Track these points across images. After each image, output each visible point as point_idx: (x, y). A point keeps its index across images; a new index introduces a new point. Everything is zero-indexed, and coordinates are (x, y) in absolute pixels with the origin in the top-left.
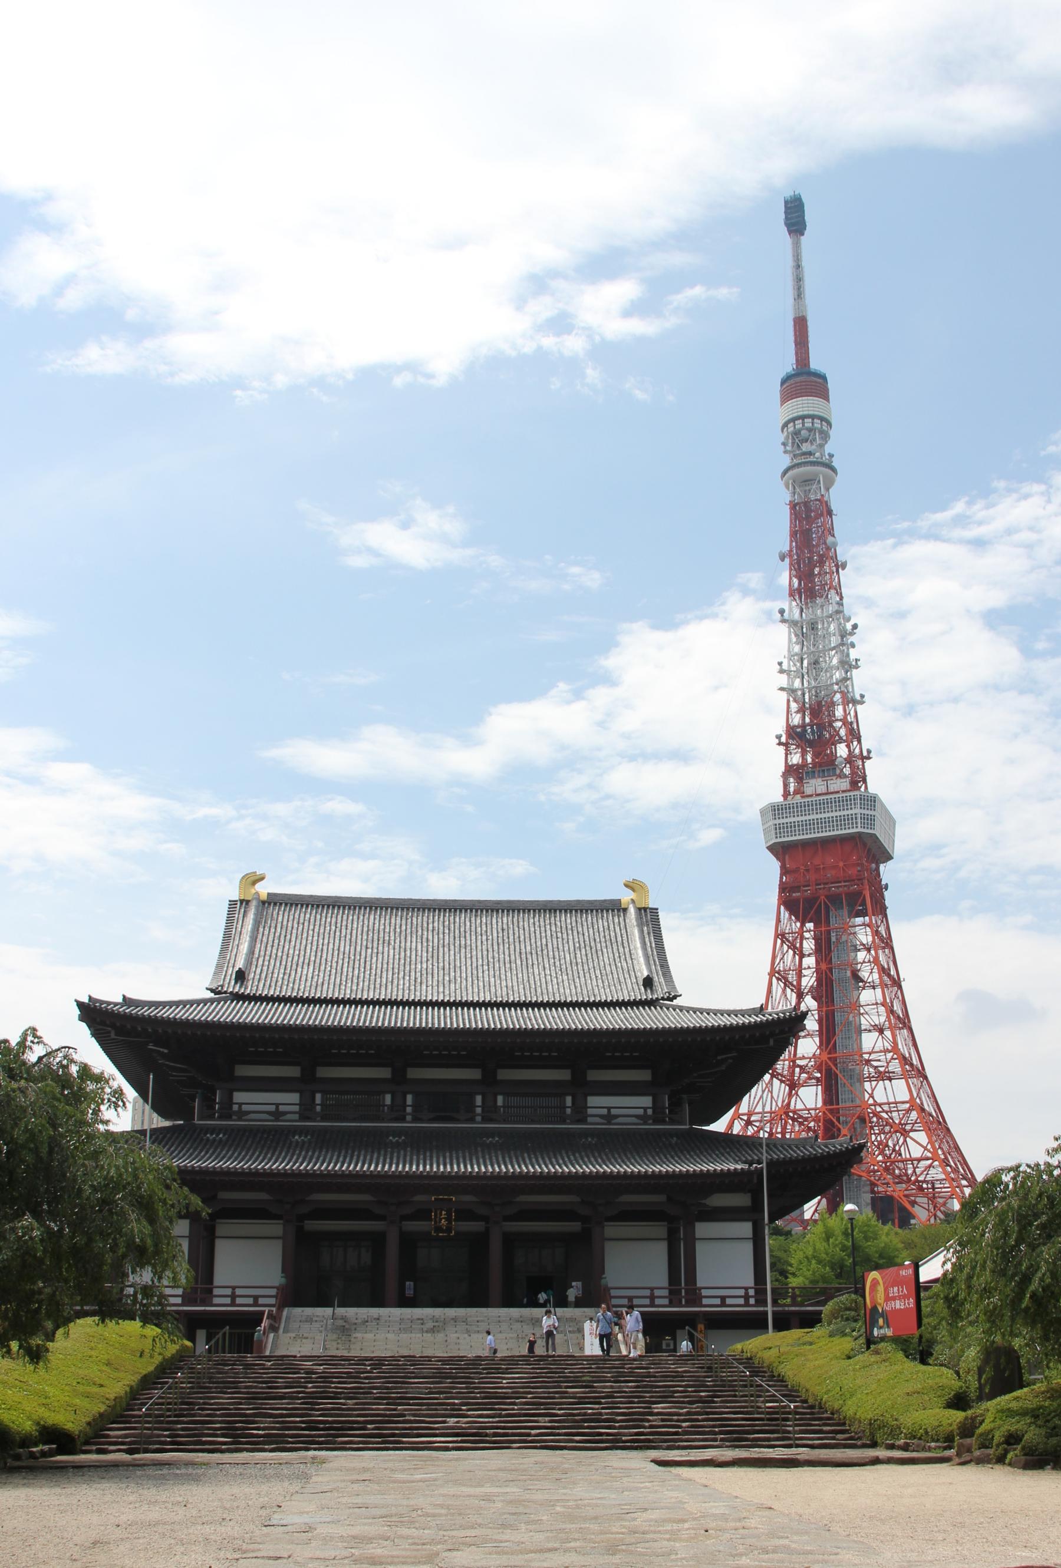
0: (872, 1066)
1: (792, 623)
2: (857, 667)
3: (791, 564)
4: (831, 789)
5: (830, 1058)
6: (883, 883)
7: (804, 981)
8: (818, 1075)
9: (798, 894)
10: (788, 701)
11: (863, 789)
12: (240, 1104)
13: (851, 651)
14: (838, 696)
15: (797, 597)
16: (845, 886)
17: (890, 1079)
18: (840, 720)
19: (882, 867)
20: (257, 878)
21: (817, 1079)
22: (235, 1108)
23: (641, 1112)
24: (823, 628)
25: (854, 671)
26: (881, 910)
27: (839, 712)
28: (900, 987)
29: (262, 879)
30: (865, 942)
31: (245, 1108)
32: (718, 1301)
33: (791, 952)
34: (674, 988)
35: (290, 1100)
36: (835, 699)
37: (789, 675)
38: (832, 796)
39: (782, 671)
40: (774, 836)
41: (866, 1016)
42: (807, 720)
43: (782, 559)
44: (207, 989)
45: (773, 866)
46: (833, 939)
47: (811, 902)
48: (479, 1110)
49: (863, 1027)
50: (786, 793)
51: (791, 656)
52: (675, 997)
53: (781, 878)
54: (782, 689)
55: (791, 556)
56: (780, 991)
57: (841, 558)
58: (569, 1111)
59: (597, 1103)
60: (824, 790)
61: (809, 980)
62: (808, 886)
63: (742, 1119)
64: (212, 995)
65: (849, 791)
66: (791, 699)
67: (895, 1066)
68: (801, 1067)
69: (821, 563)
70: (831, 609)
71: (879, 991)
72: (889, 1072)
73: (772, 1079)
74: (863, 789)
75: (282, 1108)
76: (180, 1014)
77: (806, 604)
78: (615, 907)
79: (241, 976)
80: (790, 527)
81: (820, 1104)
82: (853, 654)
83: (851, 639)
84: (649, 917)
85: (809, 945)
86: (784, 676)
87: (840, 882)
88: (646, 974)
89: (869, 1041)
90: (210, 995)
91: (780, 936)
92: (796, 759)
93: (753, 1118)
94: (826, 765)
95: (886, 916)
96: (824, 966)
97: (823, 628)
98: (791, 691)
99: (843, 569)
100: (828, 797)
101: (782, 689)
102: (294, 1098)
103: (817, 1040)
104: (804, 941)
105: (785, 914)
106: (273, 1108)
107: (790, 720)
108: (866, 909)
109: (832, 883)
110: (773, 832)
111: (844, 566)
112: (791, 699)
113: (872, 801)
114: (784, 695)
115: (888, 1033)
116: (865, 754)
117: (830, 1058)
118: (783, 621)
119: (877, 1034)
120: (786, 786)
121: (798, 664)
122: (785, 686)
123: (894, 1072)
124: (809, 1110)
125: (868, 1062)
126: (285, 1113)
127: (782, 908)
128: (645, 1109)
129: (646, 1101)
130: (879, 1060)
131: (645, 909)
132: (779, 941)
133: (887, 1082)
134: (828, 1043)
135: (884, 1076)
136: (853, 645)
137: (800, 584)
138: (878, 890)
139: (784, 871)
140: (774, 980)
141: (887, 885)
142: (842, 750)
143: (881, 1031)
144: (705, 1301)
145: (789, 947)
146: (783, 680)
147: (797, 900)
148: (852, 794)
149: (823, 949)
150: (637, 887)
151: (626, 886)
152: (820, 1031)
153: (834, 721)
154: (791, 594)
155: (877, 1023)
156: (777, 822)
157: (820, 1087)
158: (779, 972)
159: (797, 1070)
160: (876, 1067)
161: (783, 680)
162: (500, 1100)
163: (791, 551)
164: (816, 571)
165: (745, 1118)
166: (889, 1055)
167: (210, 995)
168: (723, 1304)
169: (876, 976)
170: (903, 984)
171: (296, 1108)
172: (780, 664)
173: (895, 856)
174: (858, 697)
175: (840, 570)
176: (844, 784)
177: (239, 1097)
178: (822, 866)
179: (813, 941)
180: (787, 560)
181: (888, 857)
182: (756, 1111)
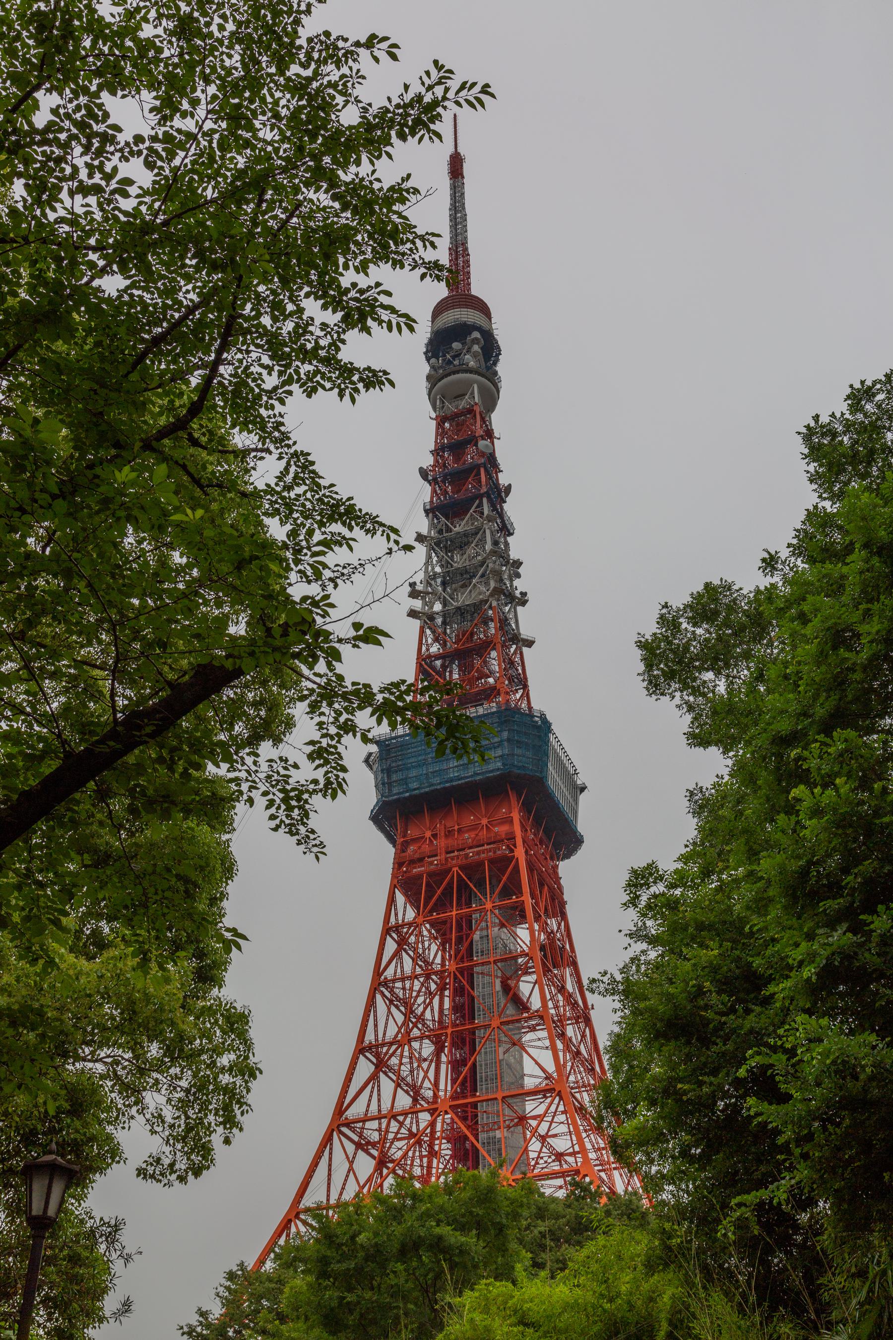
2: (523, 603)
16: (490, 850)
25: (519, 609)
28: (588, 1021)
37: (423, 598)
49: (530, 1083)
51: (430, 578)
62: (436, 855)
98: (426, 618)
99: (507, 494)
101: (413, 614)
107: (424, 648)
109: (471, 848)
114: (416, 624)
158: (385, 983)
170: (592, 1012)
178: (456, 827)
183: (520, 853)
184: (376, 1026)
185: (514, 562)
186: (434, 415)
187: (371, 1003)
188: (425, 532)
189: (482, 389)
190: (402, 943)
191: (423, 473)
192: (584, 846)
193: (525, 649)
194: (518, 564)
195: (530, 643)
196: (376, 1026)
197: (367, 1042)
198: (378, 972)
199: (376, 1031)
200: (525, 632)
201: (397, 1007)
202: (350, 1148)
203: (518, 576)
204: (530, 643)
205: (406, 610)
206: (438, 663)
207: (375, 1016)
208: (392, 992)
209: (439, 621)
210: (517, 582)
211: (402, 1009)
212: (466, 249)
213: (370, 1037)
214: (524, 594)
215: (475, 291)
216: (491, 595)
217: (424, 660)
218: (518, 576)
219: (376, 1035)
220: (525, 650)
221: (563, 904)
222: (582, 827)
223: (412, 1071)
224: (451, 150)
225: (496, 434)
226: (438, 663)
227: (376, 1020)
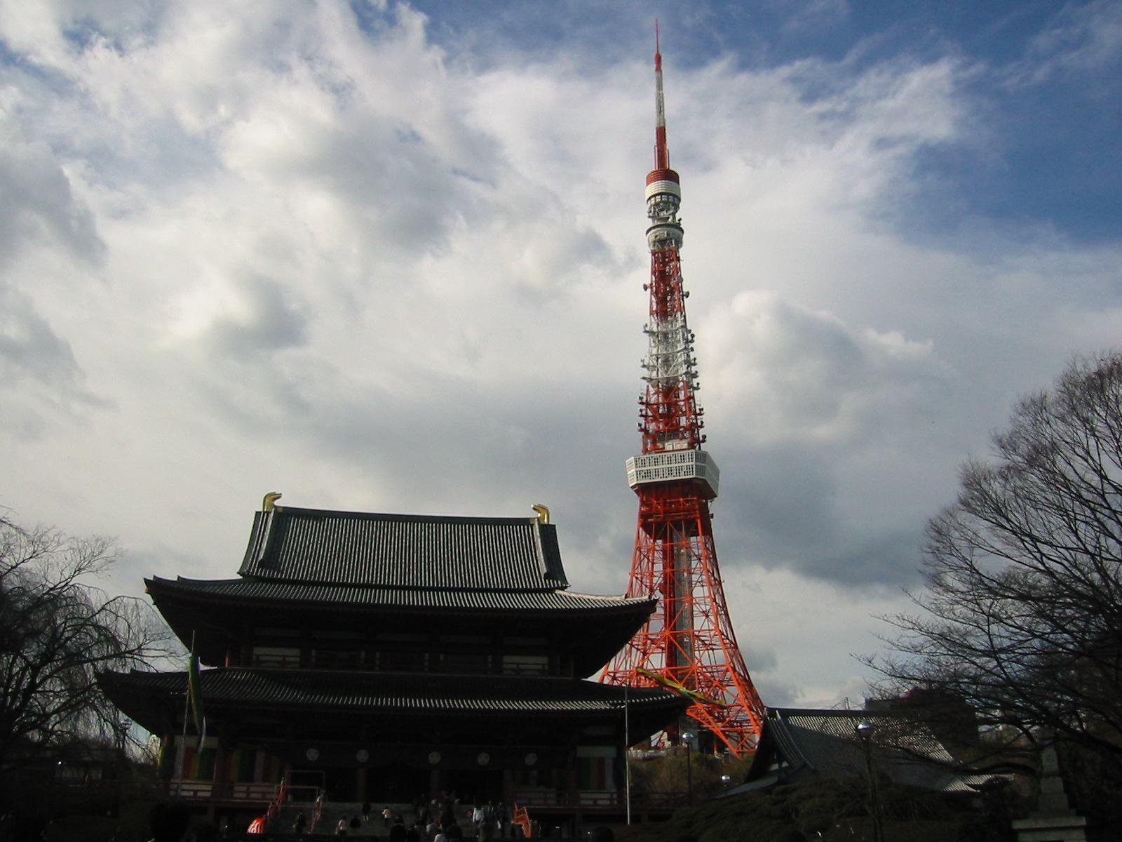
0: (700, 640)
1: (651, 333)
3: (652, 293)
4: (675, 449)
5: (671, 634)
6: (710, 513)
7: (655, 580)
8: (663, 646)
9: (652, 520)
10: (648, 386)
11: (697, 448)
12: (258, 656)
13: (691, 353)
14: (681, 384)
15: (655, 315)
17: (713, 649)
18: (683, 401)
19: (709, 504)
20: (274, 497)
21: (663, 649)
22: (254, 658)
23: (540, 667)
24: (672, 337)
26: (708, 531)
27: (682, 396)
28: (720, 584)
29: (280, 497)
30: (697, 554)
31: (262, 658)
32: (591, 802)
33: (646, 560)
34: (564, 580)
35: (292, 654)
36: (679, 386)
37: (648, 368)
38: (676, 453)
40: (635, 479)
41: (697, 605)
42: (661, 400)
44: (238, 573)
45: (635, 501)
46: (675, 551)
47: (660, 525)
48: (426, 663)
49: (694, 613)
50: (646, 451)
52: (566, 587)
53: (641, 509)
54: (644, 378)
55: (652, 288)
56: (638, 586)
57: (685, 290)
58: (490, 665)
59: (510, 661)
60: (671, 449)
61: (657, 580)
63: (610, 676)
64: (241, 577)
65: (689, 449)
66: (650, 386)
67: (717, 641)
68: (650, 639)
69: (672, 292)
70: (679, 324)
71: (706, 588)
72: (711, 644)
73: (631, 648)
74: (697, 448)
75: (287, 659)
76: (219, 591)
77: (661, 320)
78: (526, 522)
79: (262, 563)
80: (652, 268)
81: (664, 665)
82: (692, 355)
83: (691, 345)
84: (549, 533)
85: (659, 555)
86: (645, 369)
87: (680, 512)
88: (545, 571)
89: (699, 623)
90: (240, 577)
91: (639, 549)
92: (652, 427)
93: (617, 675)
94: (673, 432)
95: (711, 536)
96: (668, 570)
97: (672, 337)
99: (687, 297)
100: (674, 453)
101: (644, 378)
102: (296, 652)
103: (663, 621)
104: (656, 553)
105: (643, 534)
106: (280, 659)
107: (649, 400)
108: (698, 531)
110: (635, 476)
111: (687, 295)
112: (650, 386)
113: (702, 457)
114: (645, 381)
115: (712, 618)
116: (699, 424)
117: (671, 634)
118: (646, 332)
119: (704, 618)
120: (645, 444)
121: (655, 362)
122: (646, 376)
123: (715, 645)
124: (656, 670)
125: (698, 636)
126: (290, 663)
127: (641, 529)
128: (543, 665)
129: (543, 660)
130: (705, 636)
131: (548, 525)
132: (638, 553)
133: (710, 652)
134: (670, 623)
135: (709, 647)
136: (692, 349)
137: (657, 307)
138: (706, 518)
139: (643, 503)
140: (634, 579)
141: (712, 515)
142: (683, 421)
143: (707, 616)
144: (583, 802)
145: (645, 556)
146: (646, 373)
147: (651, 523)
148: (690, 451)
149: (670, 557)
150: (539, 509)
151: (534, 509)
152: (665, 615)
153: (678, 401)
154: (651, 314)
155: (704, 610)
156: (638, 469)
157: (664, 654)
159: (649, 641)
160: (703, 641)
161: (646, 373)
162: (442, 657)
163: (651, 284)
164: (669, 298)
165: (612, 674)
166: (712, 633)
167: (240, 577)
168: (595, 804)
169: (704, 577)
170: (723, 584)
171: (298, 659)
172: (643, 361)
173: (719, 495)
174: (695, 385)
175: (685, 297)
176: (684, 444)
177: (258, 650)
179: (661, 553)
180: (649, 290)
181: (713, 495)
182: (620, 669)
191: (645, 288)
214: (695, 359)
225: (681, 258)
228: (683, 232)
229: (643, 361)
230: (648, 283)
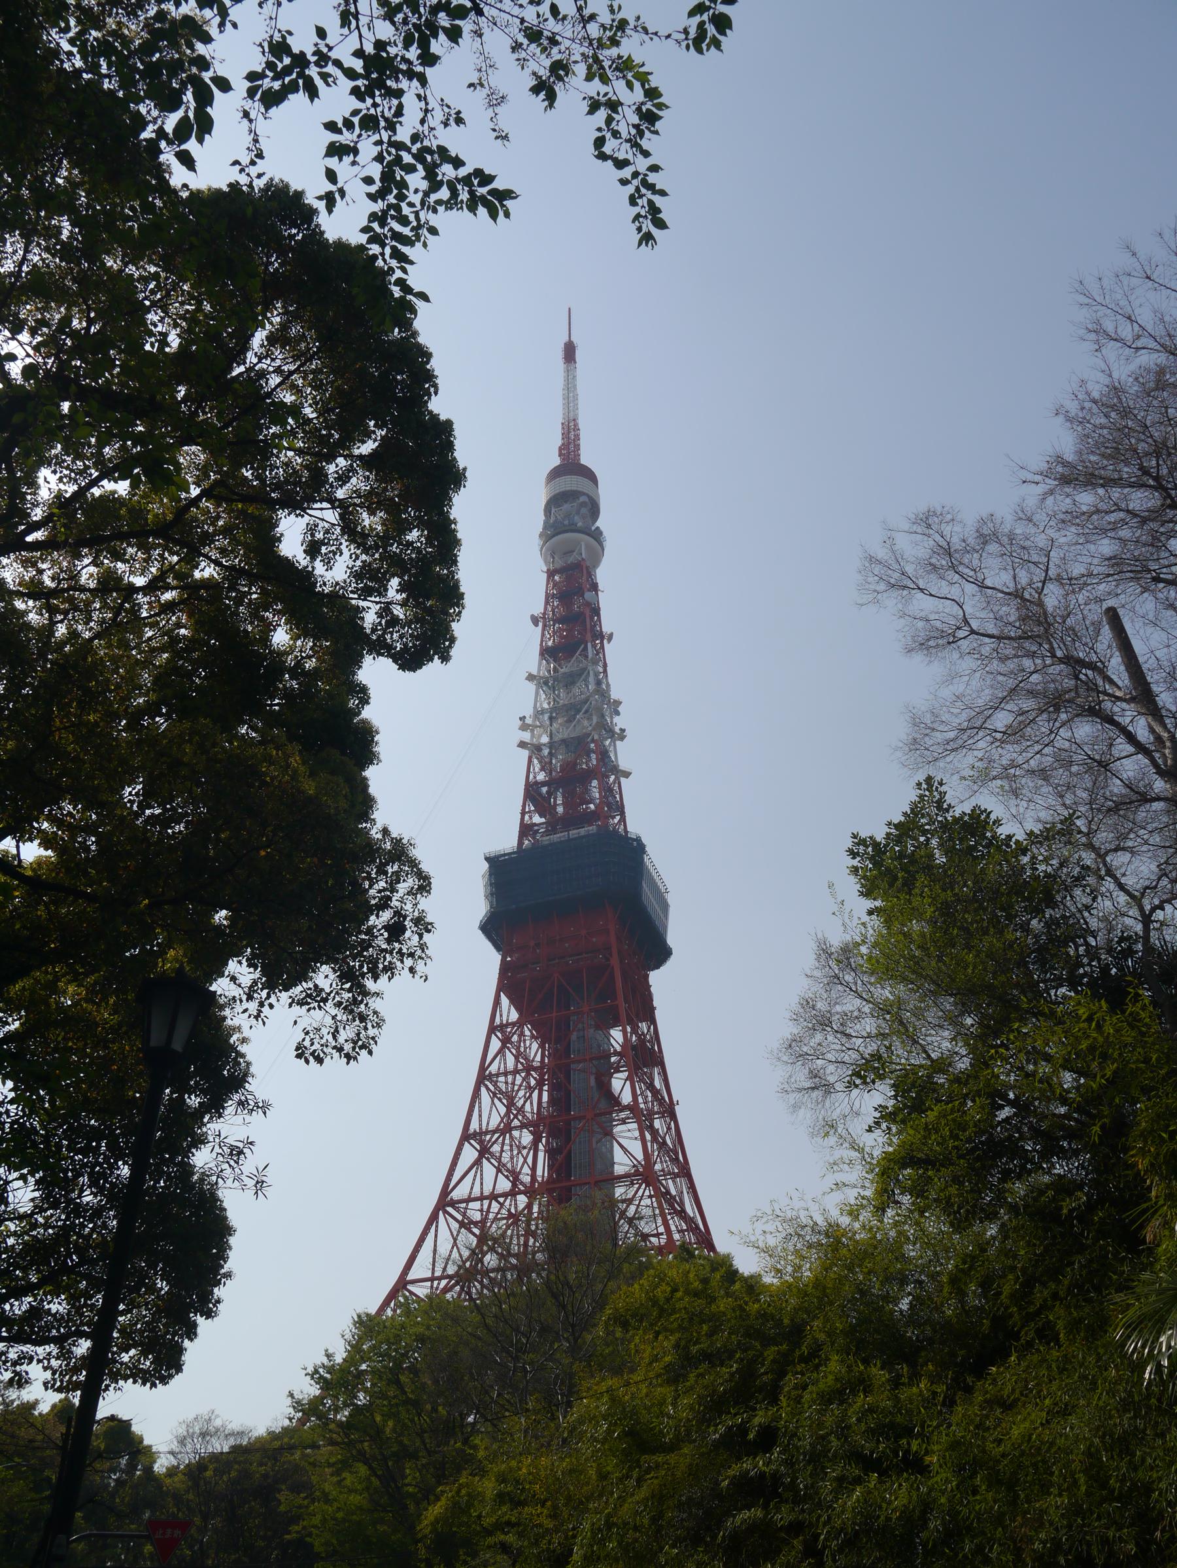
2: (622, 738)
25: (618, 743)
26: (648, 1014)
28: (673, 1117)
37: (532, 731)
39: (524, 727)
43: (536, 625)
49: (619, 1170)
51: (538, 713)
54: (522, 745)
57: (606, 629)
95: (653, 1021)
98: (536, 749)
99: (610, 640)
101: (522, 745)
107: (531, 776)
127: (503, 997)
161: (526, 736)
163: (544, 614)
170: (677, 1107)
172: (522, 719)
175: (605, 641)
180: (541, 624)
183: (615, 961)
184: (480, 1116)
185: (615, 701)
186: (545, 569)
187: (476, 1095)
188: (535, 673)
189: (588, 546)
190: (506, 1041)
191: (535, 620)
192: (672, 957)
193: (622, 780)
194: (618, 703)
195: (627, 775)
196: (480, 1116)
197: (471, 1130)
198: (483, 1068)
199: (480, 1121)
200: (623, 765)
201: (500, 1100)
202: (455, 1226)
203: (618, 713)
204: (627, 775)
205: (517, 742)
206: (544, 790)
207: (480, 1107)
208: (495, 1084)
209: (546, 752)
210: (616, 719)
211: (505, 1101)
212: (576, 425)
213: (474, 1126)
214: (623, 730)
215: (584, 461)
216: (594, 729)
217: (531, 786)
218: (618, 713)
219: (480, 1125)
220: (622, 780)
221: (653, 1009)
222: (671, 940)
223: (512, 1158)
224: (566, 339)
226: (544, 790)
227: (480, 1111)
228: (601, 544)
229: (522, 719)
230: (539, 609)
